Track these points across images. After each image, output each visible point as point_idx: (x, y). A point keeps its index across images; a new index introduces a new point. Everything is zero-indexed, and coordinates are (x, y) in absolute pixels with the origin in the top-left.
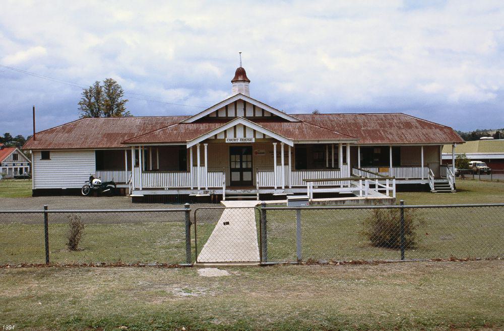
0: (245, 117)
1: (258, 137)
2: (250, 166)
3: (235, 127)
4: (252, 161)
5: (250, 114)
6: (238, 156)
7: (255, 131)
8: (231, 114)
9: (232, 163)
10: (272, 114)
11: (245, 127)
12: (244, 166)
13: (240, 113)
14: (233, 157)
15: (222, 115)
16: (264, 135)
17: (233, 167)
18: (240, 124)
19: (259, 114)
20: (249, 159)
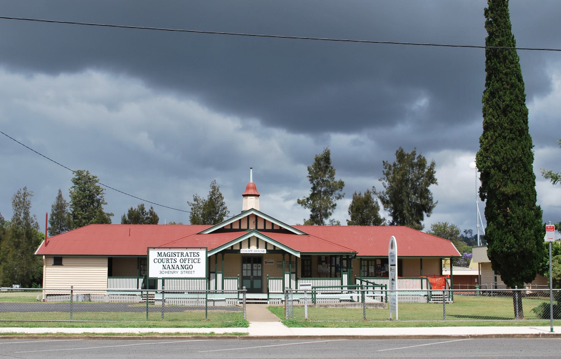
0: (257, 230)
1: (270, 248)
2: (260, 274)
3: (249, 239)
4: (262, 270)
5: (261, 226)
6: (249, 265)
7: (266, 243)
8: (244, 226)
9: (244, 271)
10: (280, 227)
11: (258, 239)
12: (255, 274)
13: (252, 227)
14: (245, 266)
15: (236, 227)
16: (274, 247)
17: (245, 274)
18: (254, 236)
19: (269, 227)
20: (260, 268)
